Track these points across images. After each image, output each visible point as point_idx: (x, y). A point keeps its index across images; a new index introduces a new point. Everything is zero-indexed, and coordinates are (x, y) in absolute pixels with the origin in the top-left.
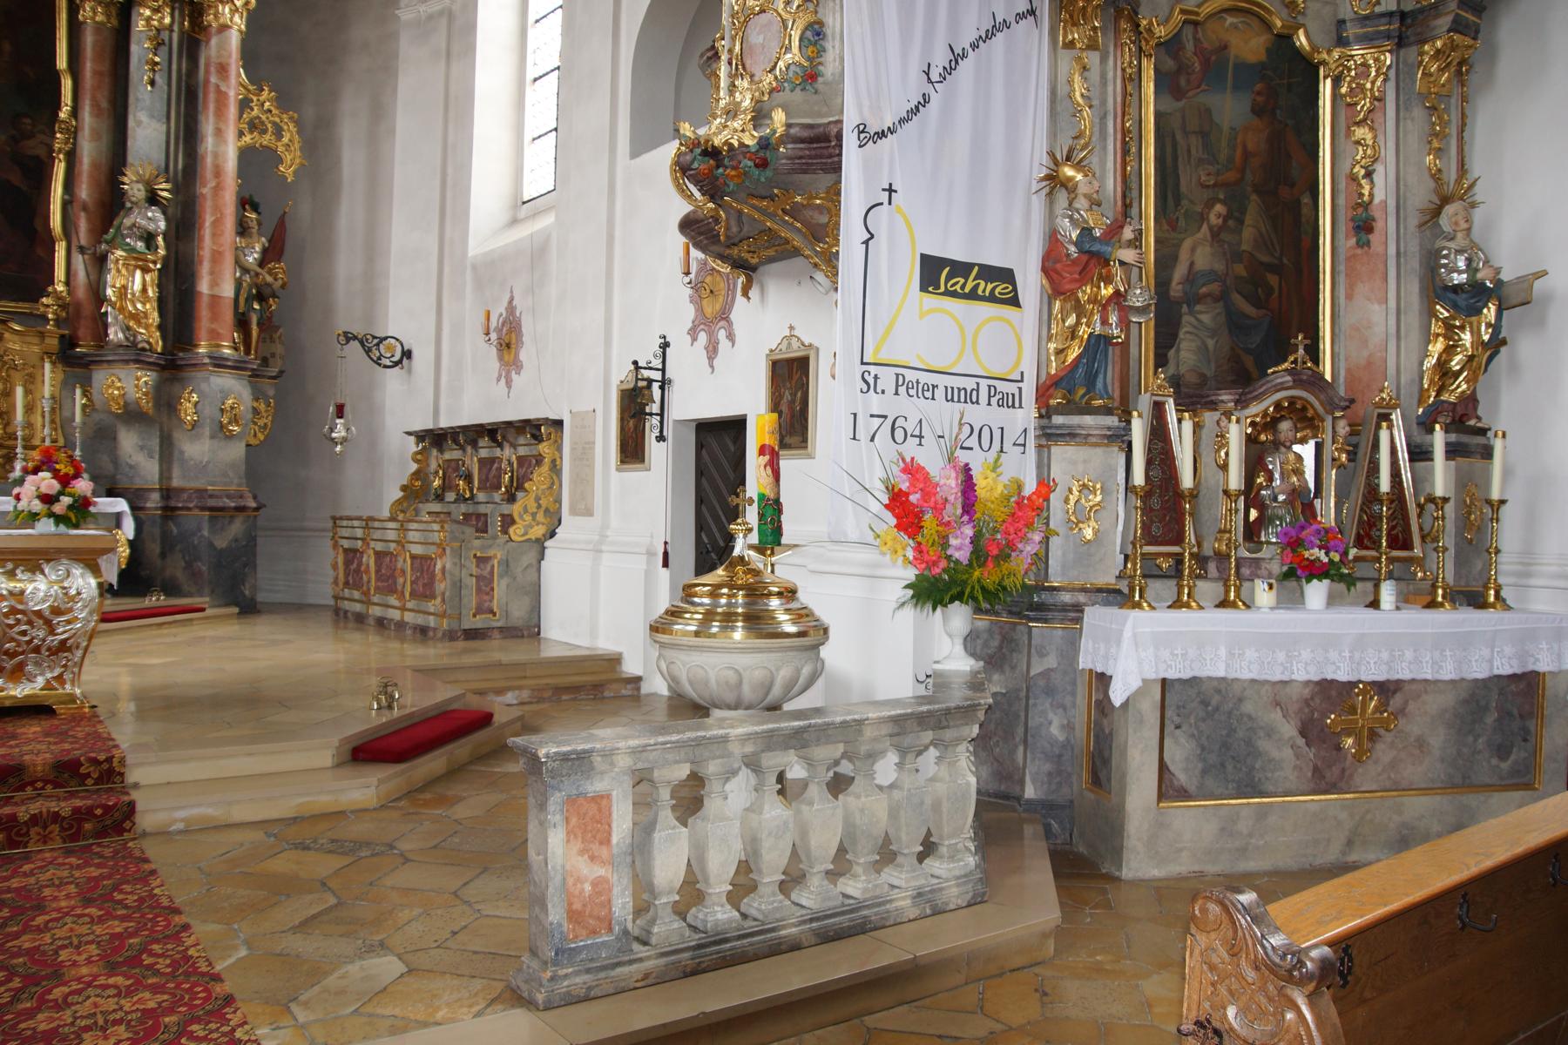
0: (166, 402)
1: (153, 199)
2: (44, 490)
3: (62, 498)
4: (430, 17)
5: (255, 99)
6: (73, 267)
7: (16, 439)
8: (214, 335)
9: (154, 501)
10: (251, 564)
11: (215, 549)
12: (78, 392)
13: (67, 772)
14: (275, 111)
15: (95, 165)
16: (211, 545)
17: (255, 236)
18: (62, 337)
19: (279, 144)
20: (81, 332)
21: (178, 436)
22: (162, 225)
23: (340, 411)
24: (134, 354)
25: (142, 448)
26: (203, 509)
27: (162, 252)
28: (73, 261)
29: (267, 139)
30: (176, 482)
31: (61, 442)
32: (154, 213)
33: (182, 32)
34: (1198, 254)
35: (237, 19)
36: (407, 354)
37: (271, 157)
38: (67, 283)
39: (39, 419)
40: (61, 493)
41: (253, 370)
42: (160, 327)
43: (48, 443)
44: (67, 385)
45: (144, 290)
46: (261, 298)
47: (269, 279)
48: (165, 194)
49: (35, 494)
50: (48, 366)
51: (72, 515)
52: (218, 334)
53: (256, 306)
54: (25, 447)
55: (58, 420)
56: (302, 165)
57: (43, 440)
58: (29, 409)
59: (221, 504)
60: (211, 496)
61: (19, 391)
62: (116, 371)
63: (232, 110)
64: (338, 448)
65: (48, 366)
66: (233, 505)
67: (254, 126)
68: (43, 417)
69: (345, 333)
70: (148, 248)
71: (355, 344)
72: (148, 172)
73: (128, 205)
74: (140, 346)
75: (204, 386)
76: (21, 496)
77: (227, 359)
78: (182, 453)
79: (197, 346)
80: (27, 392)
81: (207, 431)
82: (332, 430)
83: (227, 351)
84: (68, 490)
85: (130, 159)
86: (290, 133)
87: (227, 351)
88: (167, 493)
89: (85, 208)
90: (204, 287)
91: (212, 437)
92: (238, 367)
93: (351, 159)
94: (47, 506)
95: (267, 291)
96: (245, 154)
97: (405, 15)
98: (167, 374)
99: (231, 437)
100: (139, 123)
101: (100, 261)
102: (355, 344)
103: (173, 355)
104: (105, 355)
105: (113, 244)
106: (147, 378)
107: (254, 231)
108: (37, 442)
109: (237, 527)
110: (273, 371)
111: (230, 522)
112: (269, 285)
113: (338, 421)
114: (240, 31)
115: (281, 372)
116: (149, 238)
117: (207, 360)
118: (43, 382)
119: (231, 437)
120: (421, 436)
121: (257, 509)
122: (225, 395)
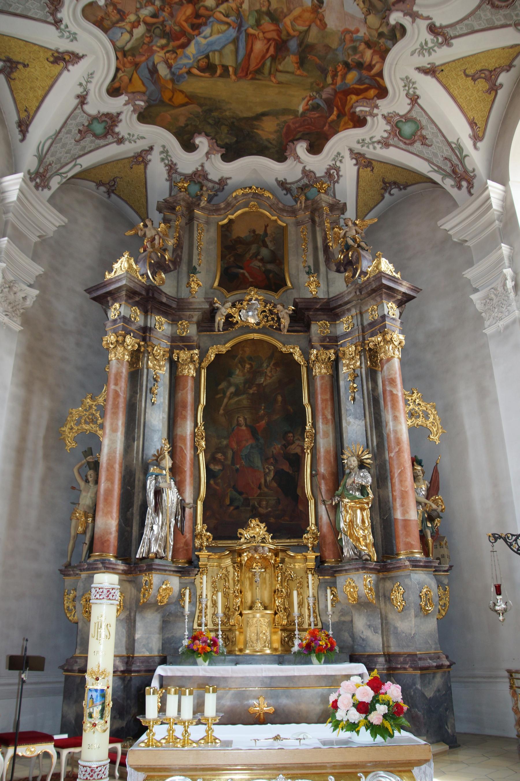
1: (362, 466)
2: (360, 698)
3: (377, 706)
4: (507, 327)
5: (410, 399)
6: (320, 514)
7: (294, 625)
10: (450, 708)
11: (427, 698)
12: (329, 591)
14: (422, 404)
16: (423, 695)
17: (422, 481)
18: (316, 557)
19: (428, 422)
20: (327, 554)
21: (392, 617)
22: (370, 479)
23: (498, 590)
25: (369, 626)
26: (415, 669)
27: (371, 496)
28: (319, 510)
29: (420, 421)
30: (393, 650)
31: (320, 626)
32: (364, 473)
33: (366, 366)
35: (397, 352)
38: (317, 524)
39: (307, 611)
40: (375, 700)
41: (435, 567)
42: (374, 545)
43: (312, 627)
44: (322, 586)
45: (363, 522)
47: (434, 506)
48: (369, 461)
49: (352, 701)
50: (310, 576)
51: (387, 724)
52: (412, 545)
53: (429, 525)
54: (299, 630)
55: (317, 611)
56: (443, 432)
57: (310, 625)
58: (301, 605)
59: (427, 665)
60: (420, 659)
61: (295, 593)
62: (351, 576)
63: (401, 404)
64: (501, 618)
65: (310, 576)
66: (435, 664)
68: (309, 609)
69: (493, 535)
70: (362, 494)
71: (500, 541)
73: (347, 471)
74: (364, 558)
75: (407, 581)
76: (339, 704)
77: (420, 561)
78: (396, 628)
79: (398, 554)
80: (298, 594)
81: (413, 612)
82: (495, 605)
83: (418, 556)
84: (381, 697)
85: (346, 445)
87: (418, 556)
89: (324, 478)
90: (398, 515)
91: (416, 616)
92: (426, 566)
94: (364, 715)
95: (434, 514)
96: (411, 430)
97: (488, 331)
98: (381, 575)
99: (427, 614)
100: (349, 423)
101: (336, 508)
102: (500, 541)
103: (385, 562)
104: (344, 566)
105: (342, 496)
107: (421, 477)
108: (306, 626)
109: (438, 681)
110: (446, 567)
111: (434, 677)
112: (435, 510)
113: (499, 597)
114: (399, 358)
115: (451, 567)
116: (363, 489)
117: (407, 563)
118: (308, 587)
119: (427, 614)
121: (449, 666)
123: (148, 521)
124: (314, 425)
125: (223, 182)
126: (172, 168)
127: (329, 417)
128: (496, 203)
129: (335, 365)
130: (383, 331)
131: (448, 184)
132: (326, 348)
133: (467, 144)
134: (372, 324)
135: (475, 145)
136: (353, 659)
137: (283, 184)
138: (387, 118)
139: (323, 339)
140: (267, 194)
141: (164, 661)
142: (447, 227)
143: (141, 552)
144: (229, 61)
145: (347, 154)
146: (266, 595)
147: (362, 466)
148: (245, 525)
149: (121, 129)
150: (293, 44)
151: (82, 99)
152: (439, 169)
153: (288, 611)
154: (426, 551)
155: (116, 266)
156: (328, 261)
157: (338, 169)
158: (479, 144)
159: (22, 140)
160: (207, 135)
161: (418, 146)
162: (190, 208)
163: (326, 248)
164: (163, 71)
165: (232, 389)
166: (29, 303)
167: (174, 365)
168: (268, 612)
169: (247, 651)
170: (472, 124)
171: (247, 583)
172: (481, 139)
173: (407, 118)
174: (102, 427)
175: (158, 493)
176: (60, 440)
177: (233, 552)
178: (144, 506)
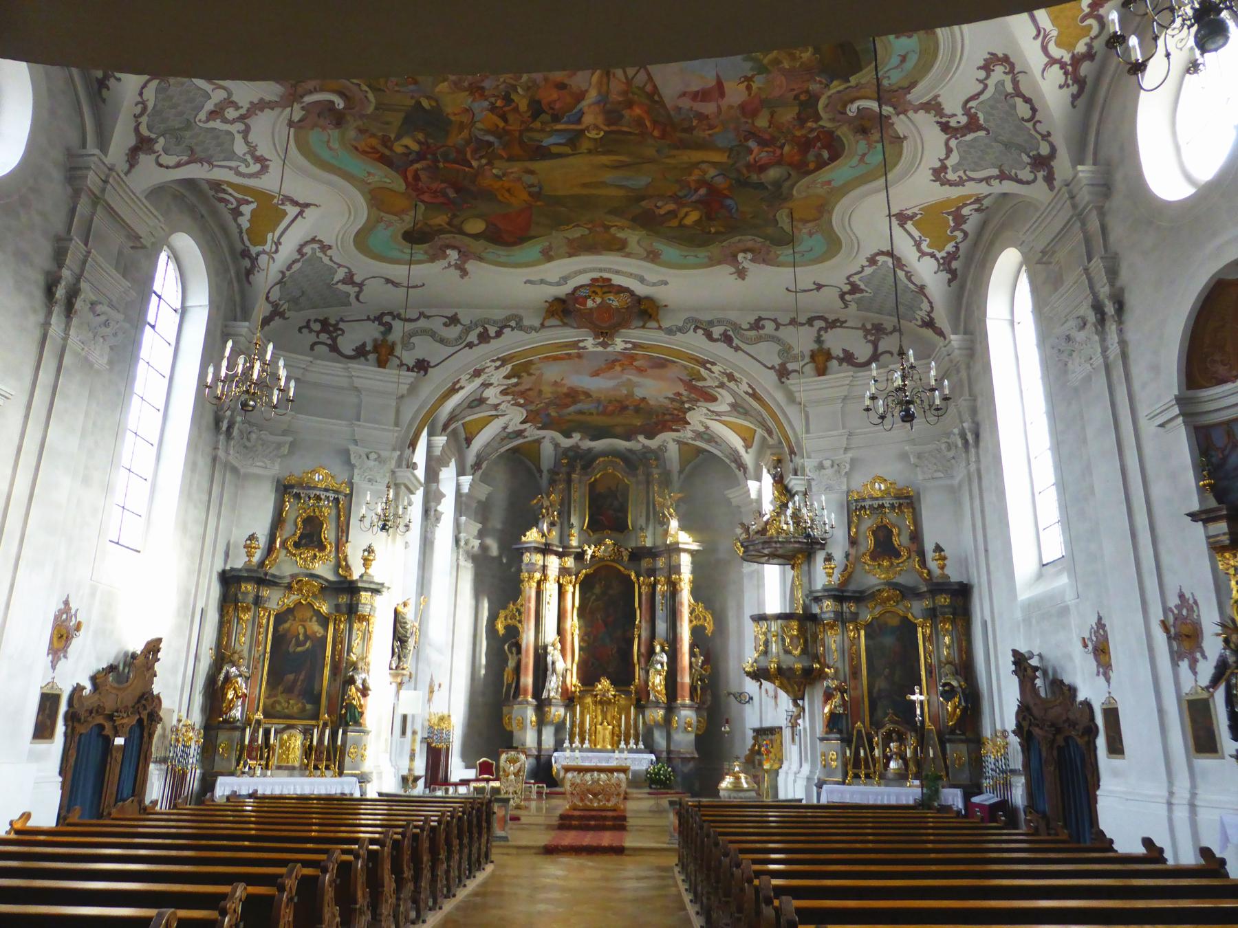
0: (667, 720)
8: (683, 697)
9: (664, 755)
13: (614, 818)
15: (646, 640)
21: (673, 732)
23: (727, 722)
24: (657, 704)
27: (666, 668)
29: (701, 622)
30: (672, 748)
34: (881, 684)
36: (751, 698)
37: (704, 628)
42: (667, 694)
46: (701, 680)
67: (697, 617)
72: (662, 641)
86: (709, 617)
88: (669, 752)
92: (690, 707)
93: (732, 625)
101: (647, 672)
106: (661, 712)
109: (691, 765)
119: (689, 732)
120: (755, 730)
122: (686, 717)
123: (548, 679)
124: (640, 621)
125: (590, 450)
126: (557, 445)
127: (648, 618)
128: (753, 495)
129: (654, 586)
130: (679, 573)
131: (733, 465)
132: (649, 577)
133: (742, 451)
134: (675, 566)
135: (747, 452)
136: (651, 753)
137: (630, 451)
138: (693, 431)
139: (648, 570)
140: (618, 460)
141: (556, 750)
142: (730, 496)
143: (544, 695)
144: (594, 411)
145: (671, 442)
146: (609, 718)
147: (663, 650)
148: (599, 681)
149: (526, 434)
150: (631, 408)
151: (505, 428)
152: (727, 457)
153: (620, 726)
154: (692, 699)
155: (528, 533)
156: (655, 514)
157: (666, 447)
158: (749, 450)
159: (468, 447)
160: (579, 432)
161: (713, 444)
162: (569, 474)
163: (654, 506)
164: (553, 414)
165: (594, 597)
166: (476, 549)
167: (560, 586)
168: (610, 727)
169: (599, 747)
170: (744, 440)
171: (599, 711)
172: (750, 447)
173: (704, 433)
174: (520, 621)
175: (553, 663)
176: (497, 631)
177: (592, 695)
178: (546, 670)
